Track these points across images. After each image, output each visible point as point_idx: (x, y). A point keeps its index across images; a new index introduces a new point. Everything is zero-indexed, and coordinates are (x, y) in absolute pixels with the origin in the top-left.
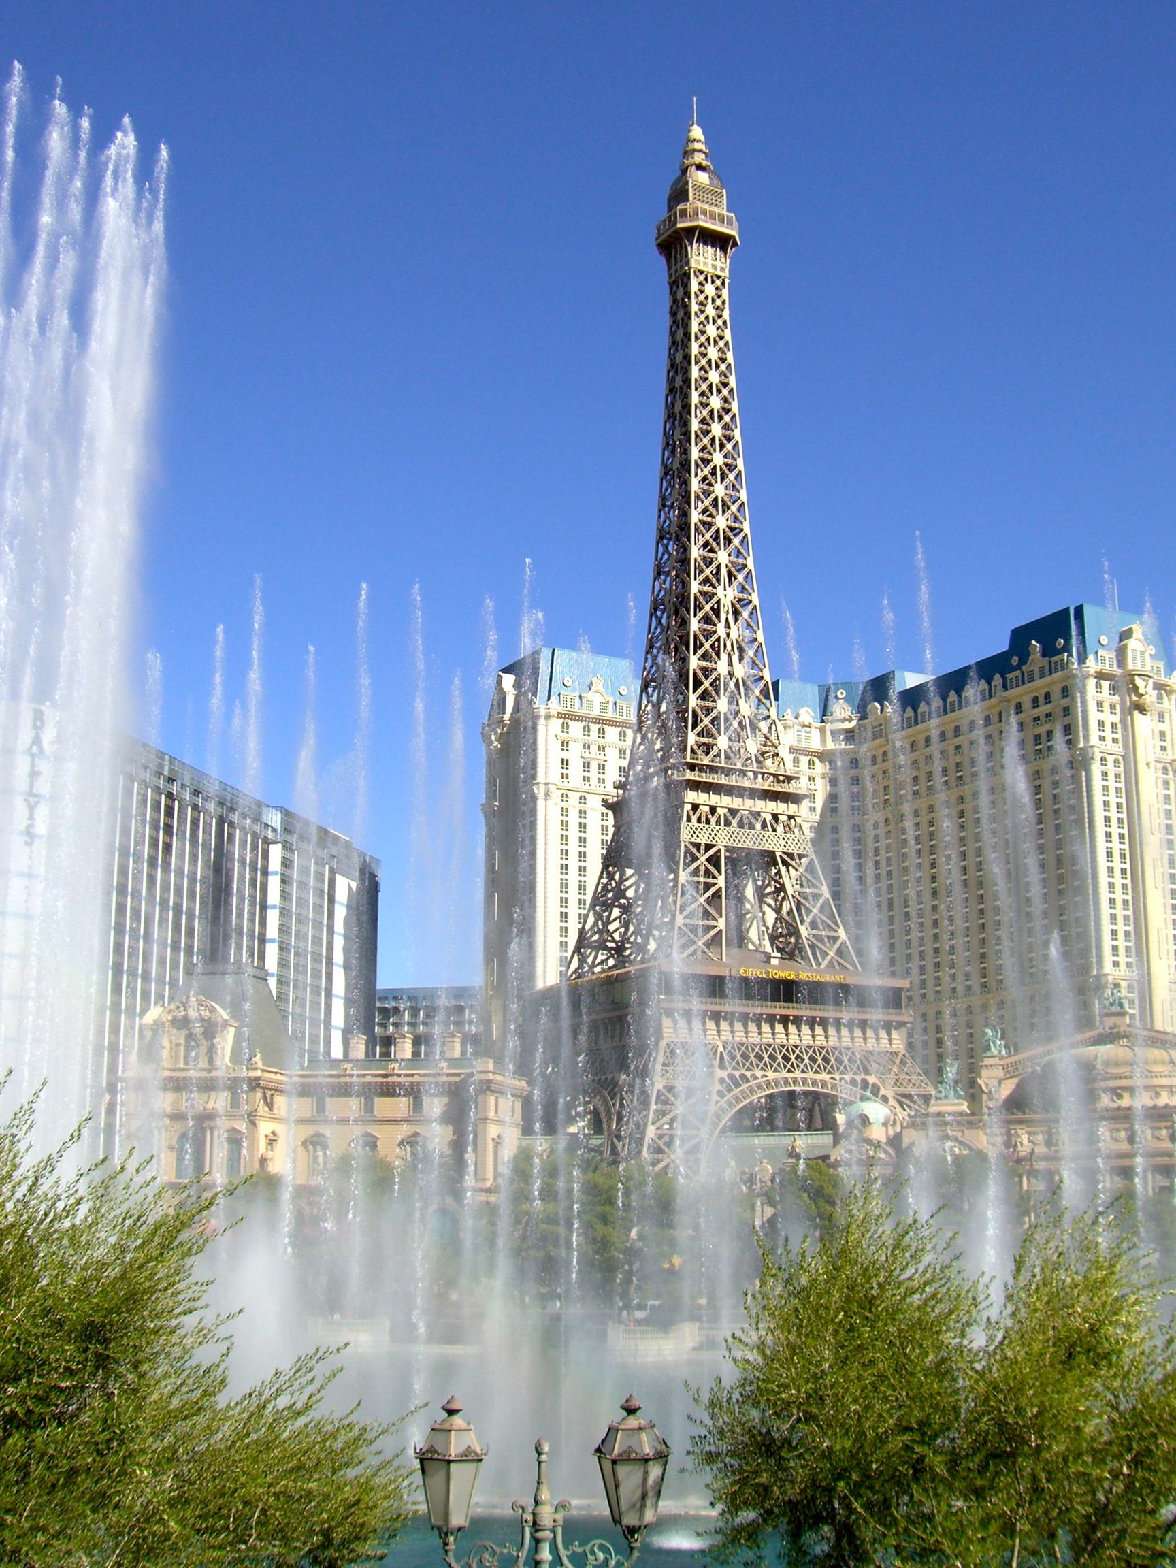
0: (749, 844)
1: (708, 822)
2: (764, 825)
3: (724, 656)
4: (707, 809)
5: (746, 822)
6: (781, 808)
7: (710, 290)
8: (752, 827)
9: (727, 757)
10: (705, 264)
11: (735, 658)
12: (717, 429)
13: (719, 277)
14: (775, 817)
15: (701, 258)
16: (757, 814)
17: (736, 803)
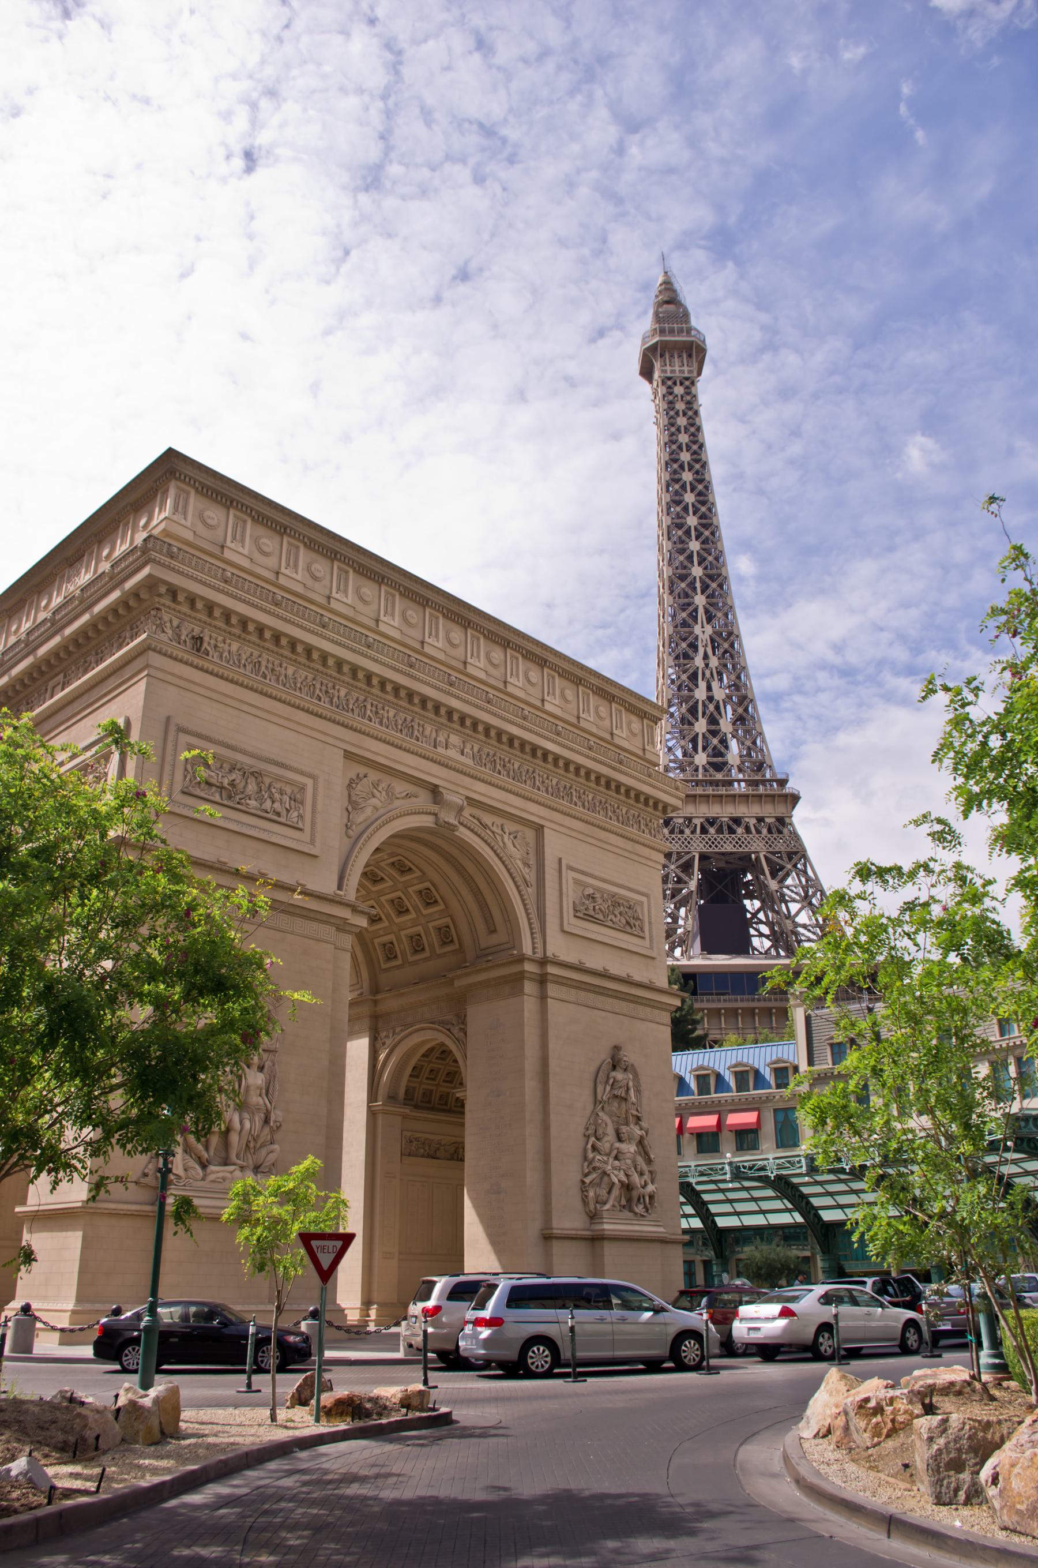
0: (729, 848)
1: (682, 832)
2: (748, 830)
3: (702, 685)
4: (681, 821)
5: (725, 828)
6: (769, 812)
7: (679, 390)
8: (732, 831)
9: (705, 770)
10: (673, 371)
11: (715, 685)
12: (689, 498)
13: (687, 379)
14: (760, 820)
15: (668, 368)
16: (737, 821)
17: (715, 810)
